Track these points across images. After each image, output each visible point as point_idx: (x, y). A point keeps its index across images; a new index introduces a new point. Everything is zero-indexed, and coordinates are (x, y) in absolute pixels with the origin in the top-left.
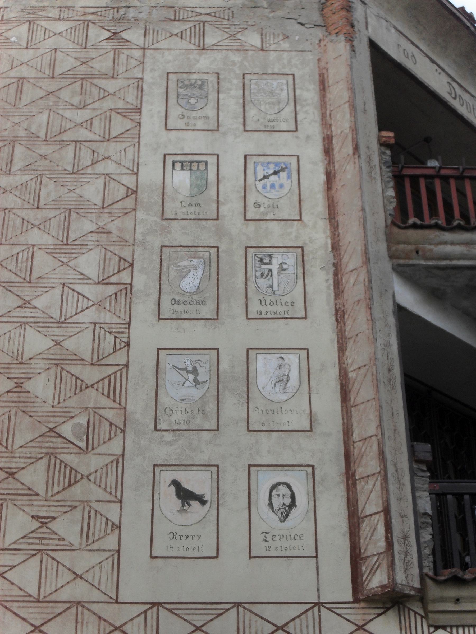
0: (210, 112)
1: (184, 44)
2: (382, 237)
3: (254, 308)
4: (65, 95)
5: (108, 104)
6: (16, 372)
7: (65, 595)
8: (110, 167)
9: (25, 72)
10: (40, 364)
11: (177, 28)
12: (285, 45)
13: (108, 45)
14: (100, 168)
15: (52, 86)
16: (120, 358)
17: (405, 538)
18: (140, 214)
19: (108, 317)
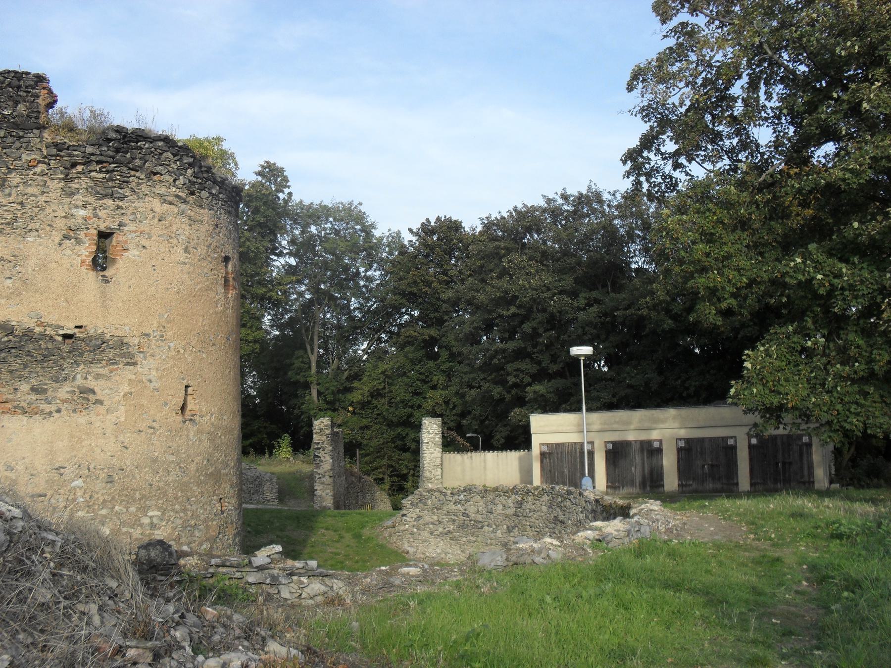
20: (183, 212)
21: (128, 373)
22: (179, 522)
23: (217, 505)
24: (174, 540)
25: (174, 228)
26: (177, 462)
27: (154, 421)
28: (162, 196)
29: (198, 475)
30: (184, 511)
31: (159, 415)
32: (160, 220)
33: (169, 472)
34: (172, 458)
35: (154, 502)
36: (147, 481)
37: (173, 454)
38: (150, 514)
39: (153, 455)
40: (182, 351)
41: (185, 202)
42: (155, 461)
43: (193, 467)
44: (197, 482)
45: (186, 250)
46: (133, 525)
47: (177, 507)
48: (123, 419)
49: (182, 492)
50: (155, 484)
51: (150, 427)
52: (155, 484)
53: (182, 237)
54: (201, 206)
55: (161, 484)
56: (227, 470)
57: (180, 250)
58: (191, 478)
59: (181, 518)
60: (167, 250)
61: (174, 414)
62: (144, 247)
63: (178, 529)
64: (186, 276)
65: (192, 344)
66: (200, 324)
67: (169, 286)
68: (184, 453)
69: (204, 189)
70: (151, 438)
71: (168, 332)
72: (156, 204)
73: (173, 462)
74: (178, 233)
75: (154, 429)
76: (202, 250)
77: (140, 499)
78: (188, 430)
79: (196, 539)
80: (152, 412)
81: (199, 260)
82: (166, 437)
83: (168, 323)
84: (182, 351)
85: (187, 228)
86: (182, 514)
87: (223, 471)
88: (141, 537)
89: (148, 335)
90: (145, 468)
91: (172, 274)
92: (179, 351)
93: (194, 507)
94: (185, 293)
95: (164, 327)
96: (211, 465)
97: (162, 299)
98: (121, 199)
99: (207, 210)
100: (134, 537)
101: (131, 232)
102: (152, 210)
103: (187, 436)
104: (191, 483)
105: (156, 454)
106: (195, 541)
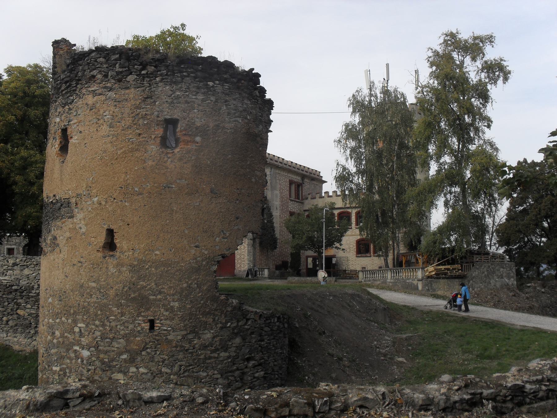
20: (109, 98)
21: (69, 223)
22: (98, 333)
23: (143, 325)
24: (94, 347)
25: (101, 112)
26: (98, 289)
27: (82, 257)
28: (94, 91)
29: (117, 299)
30: (103, 325)
31: (85, 252)
32: (91, 110)
33: (91, 295)
34: (94, 285)
35: (81, 317)
36: (77, 301)
37: (94, 282)
38: (79, 325)
39: (80, 282)
40: (103, 203)
41: (111, 89)
42: (82, 286)
43: (112, 293)
44: (116, 305)
45: (111, 126)
46: (70, 332)
47: (97, 322)
48: (66, 257)
49: (101, 311)
50: (82, 303)
51: (79, 262)
52: (82, 303)
53: (108, 117)
54: (127, 88)
55: (86, 304)
56: (159, 297)
57: (105, 127)
58: (110, 301)
59: (100, 331)
60: (95, 129)
61: (95, 252)
62: (81, 132)
63: (98, 339)
64: (109, 145)
65: (113, 196)
66: (122, 180)
67: (95, 156)
68: (104, 281)
69: (131, 74)
70: (79, 270)
71: (93, 190)
72: (90, 100)
73: (94, 288)
74: (105, 114)
75: (82, 263)
76: (128, 121)
77: (73, 314)
78: (107, 263)
79: (116, 349)
80: (81, 251)
81: (123, 130)
82: (89, 269)
83: (93, 183)
84: (103, 203)
85: (112, 108)
86: (101, 328)
87: (152, 297)
88: (73, 341)
89: (80, 195)
90: (76, 292)
91: (97, 146)
92: (100, 204)
93: (113, 324)
94: (107, 158)
95: (90, 187)
96: (134, 292)
97: (89, 167)
98: (71, 103)
99: (133, 90)
100: (70, 341)
101: (75, 124)
102: (86, 104)
103: (107, 268)
104: (110, 305)
105: (82, 281)
106: (113, 351)
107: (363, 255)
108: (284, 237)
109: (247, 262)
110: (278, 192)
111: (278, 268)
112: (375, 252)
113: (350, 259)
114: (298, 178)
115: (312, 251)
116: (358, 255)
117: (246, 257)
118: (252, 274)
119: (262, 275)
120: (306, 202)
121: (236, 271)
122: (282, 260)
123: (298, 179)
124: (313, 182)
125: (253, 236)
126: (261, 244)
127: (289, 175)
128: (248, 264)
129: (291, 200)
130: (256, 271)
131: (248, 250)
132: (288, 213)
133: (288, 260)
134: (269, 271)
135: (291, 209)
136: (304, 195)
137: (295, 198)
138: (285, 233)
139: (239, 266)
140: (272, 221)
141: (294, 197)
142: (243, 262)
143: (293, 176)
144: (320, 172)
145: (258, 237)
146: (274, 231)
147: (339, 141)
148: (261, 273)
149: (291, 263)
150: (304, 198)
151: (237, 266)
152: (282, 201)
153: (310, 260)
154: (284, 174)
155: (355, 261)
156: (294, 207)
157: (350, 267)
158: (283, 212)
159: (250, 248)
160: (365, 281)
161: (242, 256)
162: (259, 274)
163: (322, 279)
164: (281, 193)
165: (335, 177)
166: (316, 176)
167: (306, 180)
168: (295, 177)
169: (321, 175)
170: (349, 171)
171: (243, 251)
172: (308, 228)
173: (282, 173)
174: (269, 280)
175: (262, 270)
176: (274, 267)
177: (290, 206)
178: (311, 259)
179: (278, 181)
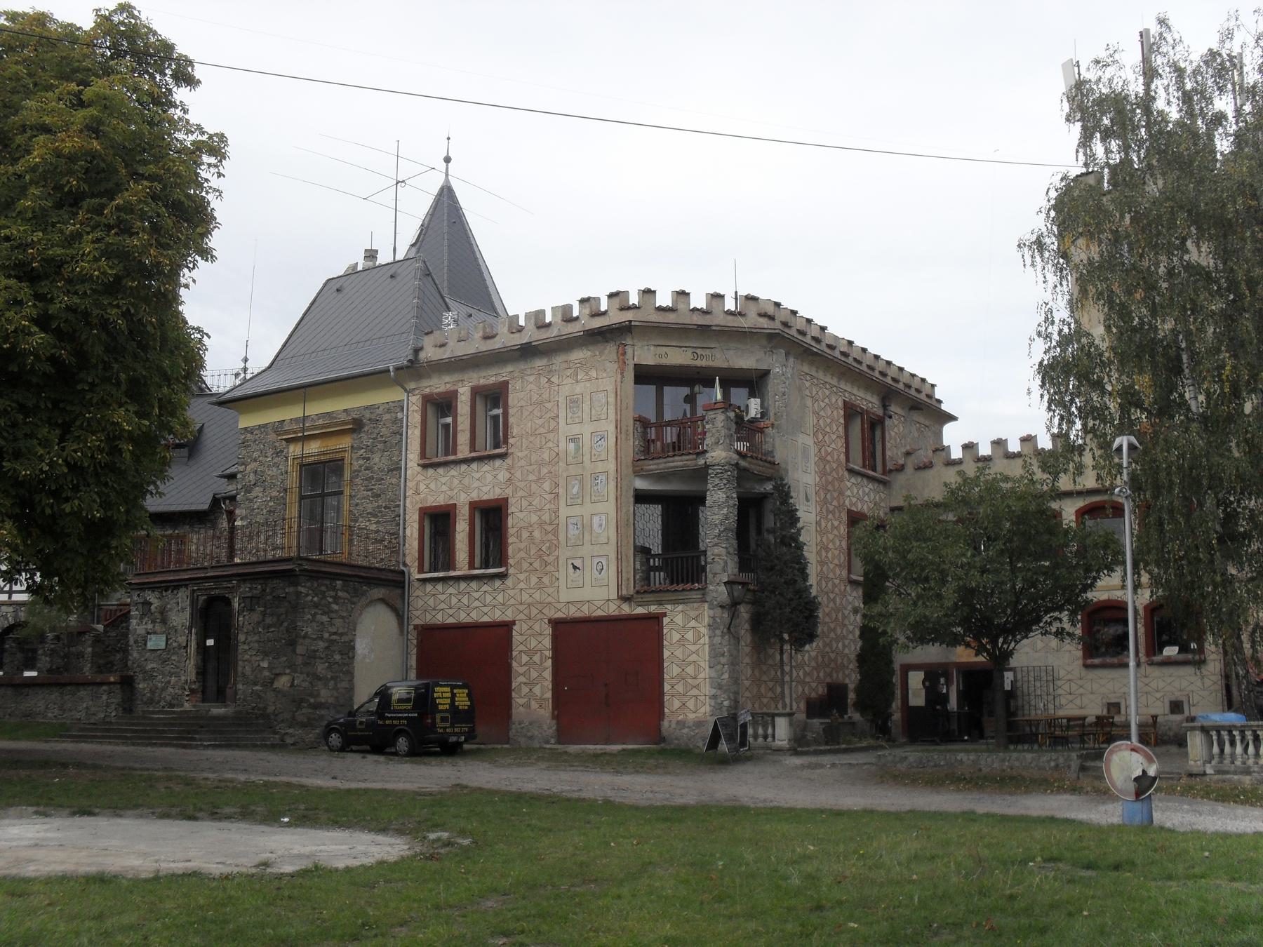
0: (580, 414)
1: (570, 380)
2: (630, 464)
3: (593, 498)
4: (535, 412)
5: (548, 415)
6: (530, 529)
7: (546, 601)
8: (550, 444)
9: (523, 403)
10: (536, 526)
11: (569, 372)
12: (605, 375)
13: (547, 385)
14: (548, 445)
15: (530, 408)
16: (556, 522)
17: (628, 579)
18: (561, 464)
19: (553, 507)
107: (1109, 660)
108: (834, 600)
109: (707, 690)
110: (810, 441)
111: (815, 708)
112: (1154, 647)
113: (1062, 673)
114: (869, 397)
115: (968, 645)
116: (1089, 661)
117: (705, 673)
118: (730, 739)
119: (765, 737)
120: (900, 480)
121: (665, 723)
122: (828, 680)
123: (869, 401)
124: (917, 416)
125: (730, 594)
126: (757, 623)
127: (843, 385)
128: (714, 697)
129: (852, 472)
130: (744, 726)
131: (712, 645)
132: (844, 517)
133: (847, 681)
134: (791, 724)
135: (852, 504)
136: (891, 458)
137: (864, 466)
138: (834, 585)
139: (677, 704)
140: (795, 538)
141: (860, 461)
142: (694, 692)
143: (855, 391)
144: (933, 386)
145: (749, 596)
146: (805, 577)
147: (1039, 244)
148: (760, 731)
149: (858, 690)
150: (890, 466)
151: (672, 704)
152: (822, 473)
153: (916, 680)
154: (828, 379)
155: (1080, 682)
156: (862, 496)
157: (1064, 701)
158: (828, 510)
159: (717, 640)
160: (1218, 772)
161: (690, 670)
162: (756, 737)
163: (1131, 787)
164: (820, 444)
165: (1041, 364)
166: (923, 397)
167: (894, 408)
168: (861, 394)
169: (937, 396)
170: (1091, 344)
171: (693, 648)
172: (964, 555)
173: (821, 375)
174: (797, 761)
175: (768, 719)
176: (803, 705)
177: (848, 493)
178: (920, 675)
179: (809, 402)
